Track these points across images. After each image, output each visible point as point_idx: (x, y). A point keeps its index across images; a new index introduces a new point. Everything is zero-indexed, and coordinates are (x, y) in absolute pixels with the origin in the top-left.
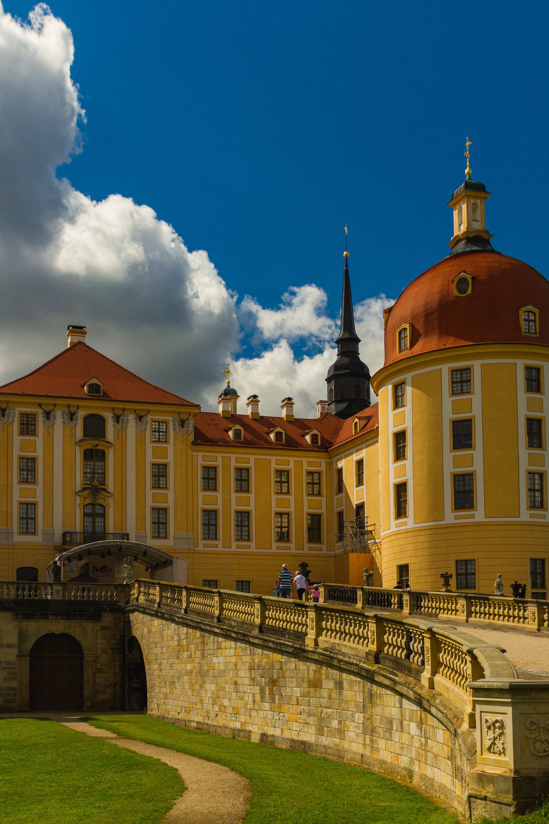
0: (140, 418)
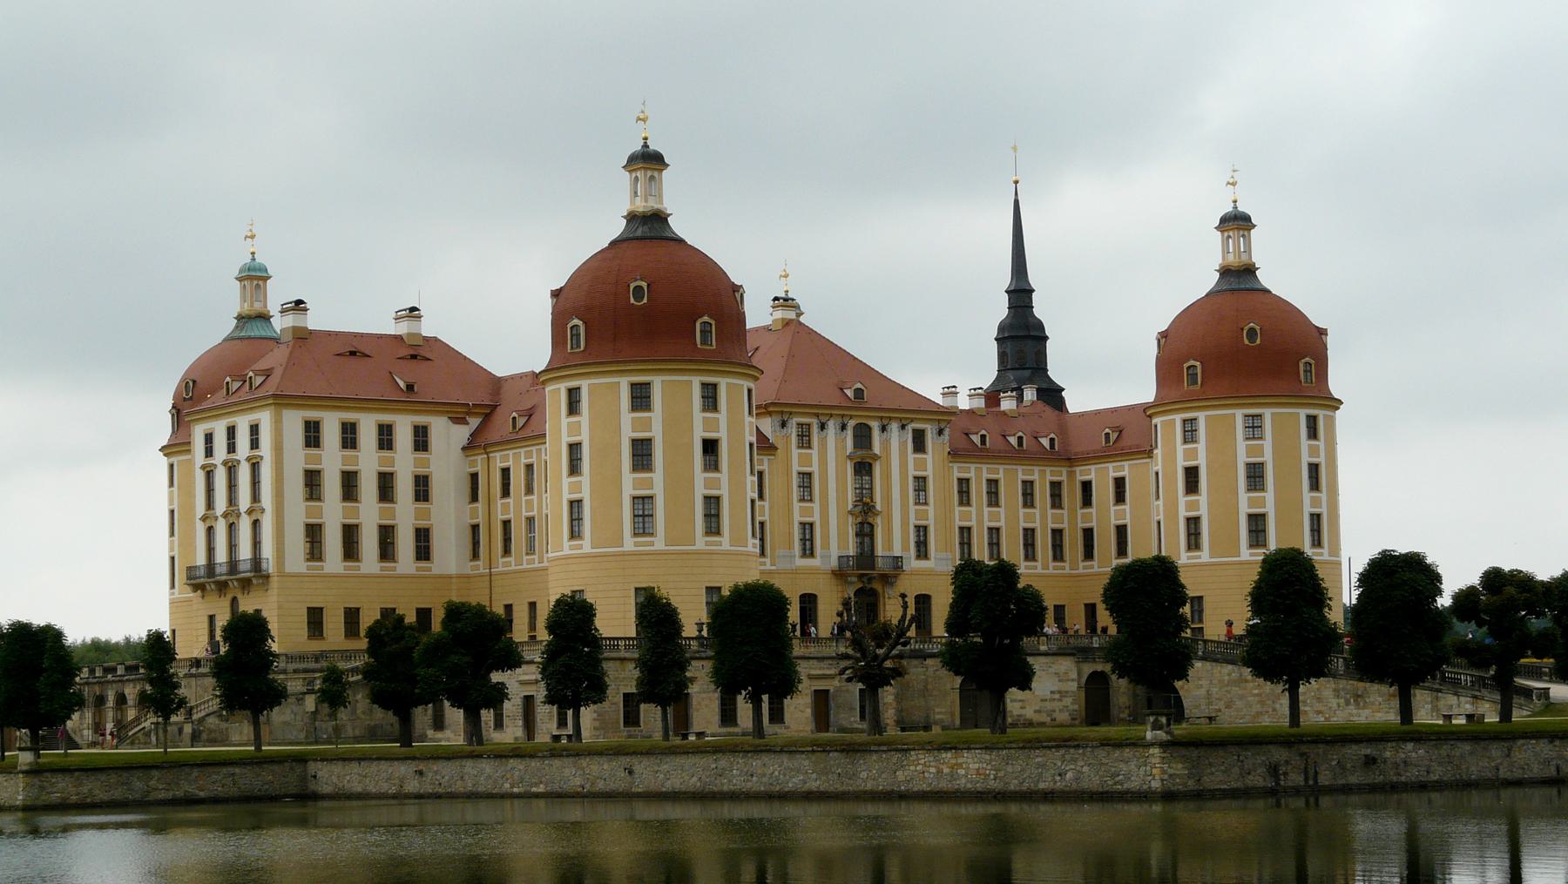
0: (903, 427)
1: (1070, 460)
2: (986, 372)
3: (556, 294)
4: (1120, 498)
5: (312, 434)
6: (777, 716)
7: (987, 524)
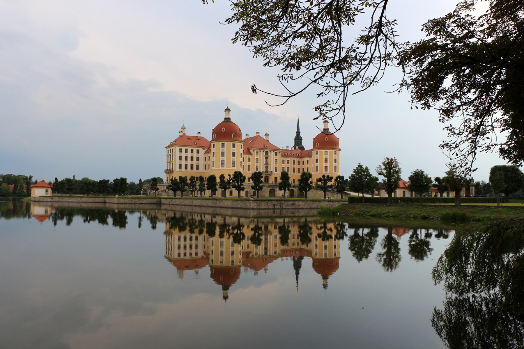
1: (301, 157)
2: (293, 144)
3: (213, 130)
4: (308, 163)
5: (181, 151)
6: (215, 194)
7: (287, 167)
